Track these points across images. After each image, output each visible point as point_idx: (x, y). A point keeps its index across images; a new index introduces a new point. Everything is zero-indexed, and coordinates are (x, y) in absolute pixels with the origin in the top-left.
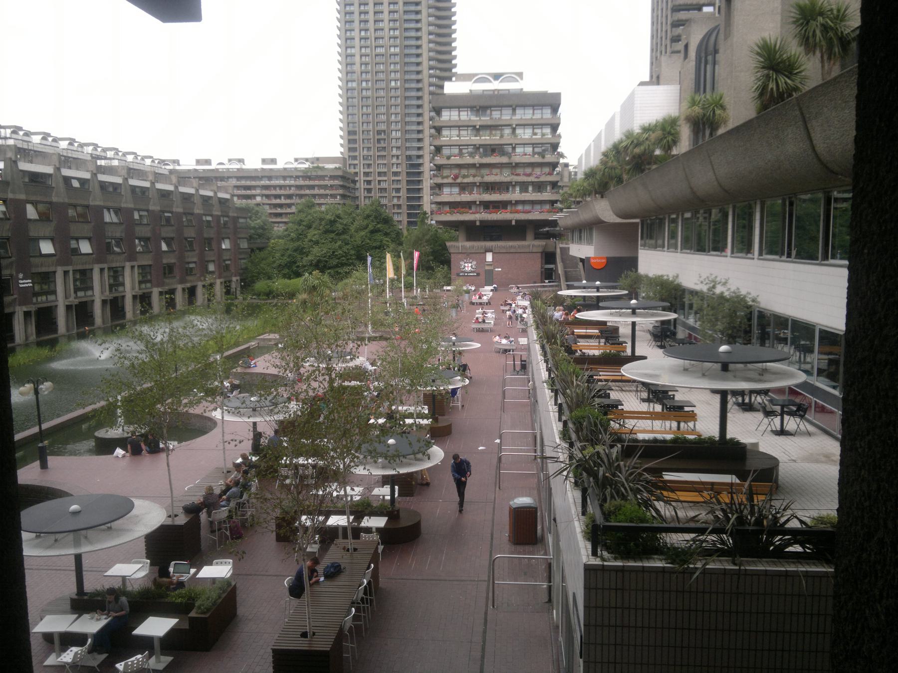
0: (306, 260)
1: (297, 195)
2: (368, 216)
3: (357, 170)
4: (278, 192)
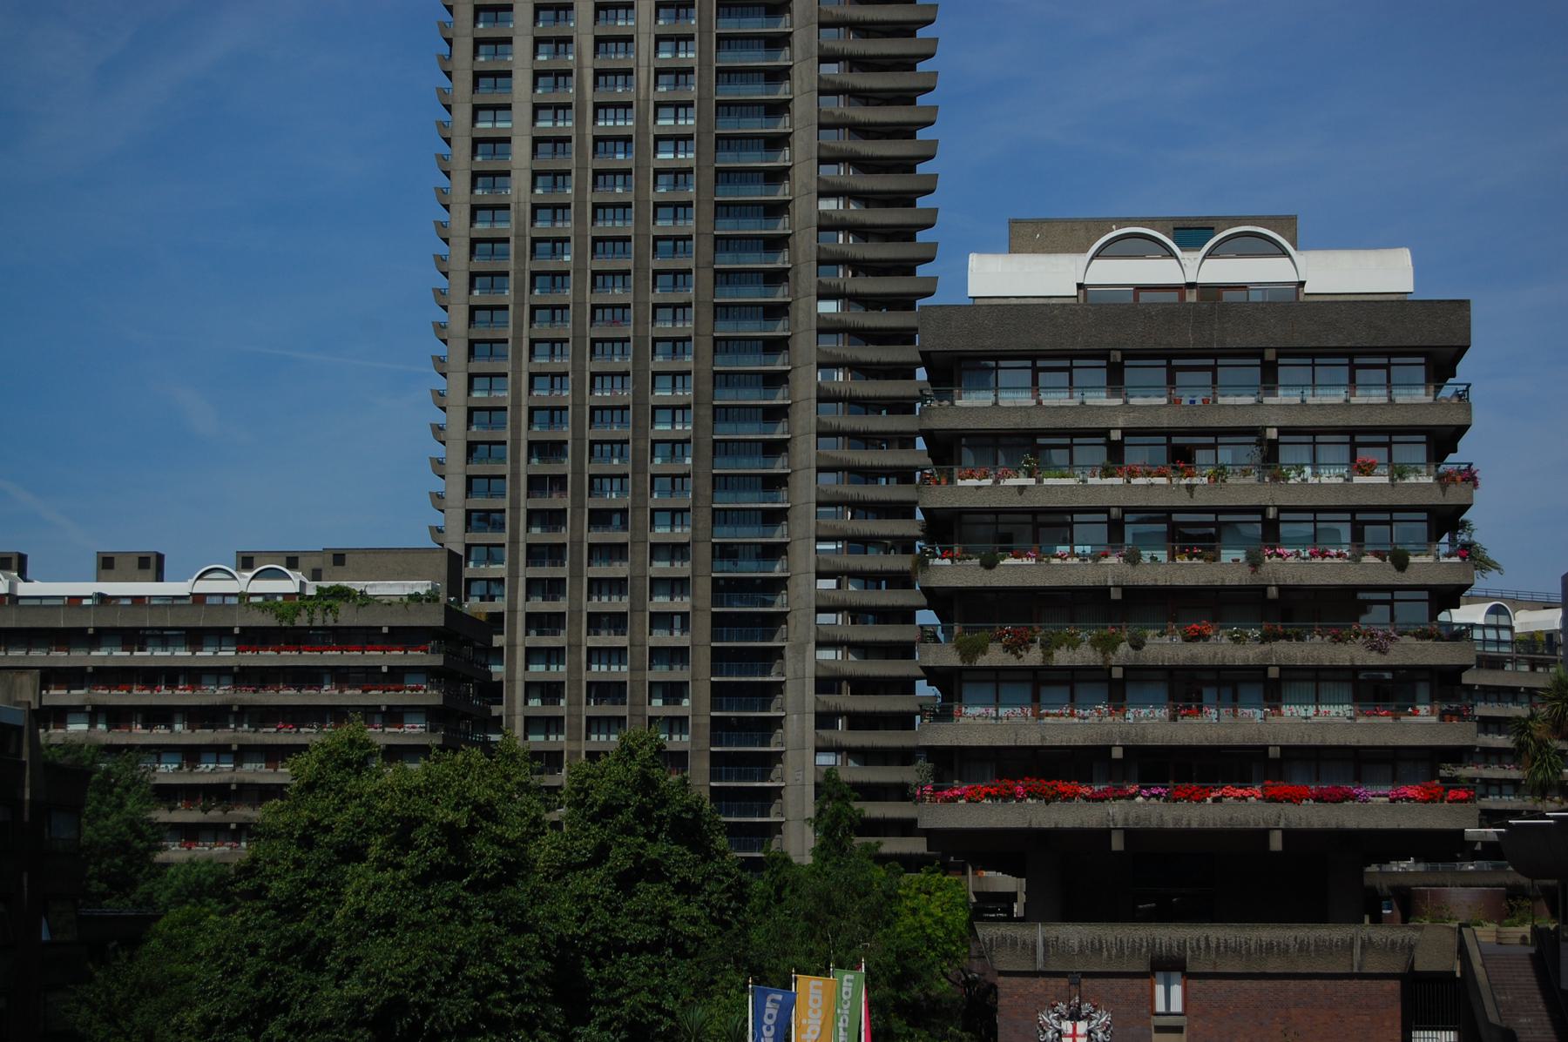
2: (610, 809)
3: (500, 605)
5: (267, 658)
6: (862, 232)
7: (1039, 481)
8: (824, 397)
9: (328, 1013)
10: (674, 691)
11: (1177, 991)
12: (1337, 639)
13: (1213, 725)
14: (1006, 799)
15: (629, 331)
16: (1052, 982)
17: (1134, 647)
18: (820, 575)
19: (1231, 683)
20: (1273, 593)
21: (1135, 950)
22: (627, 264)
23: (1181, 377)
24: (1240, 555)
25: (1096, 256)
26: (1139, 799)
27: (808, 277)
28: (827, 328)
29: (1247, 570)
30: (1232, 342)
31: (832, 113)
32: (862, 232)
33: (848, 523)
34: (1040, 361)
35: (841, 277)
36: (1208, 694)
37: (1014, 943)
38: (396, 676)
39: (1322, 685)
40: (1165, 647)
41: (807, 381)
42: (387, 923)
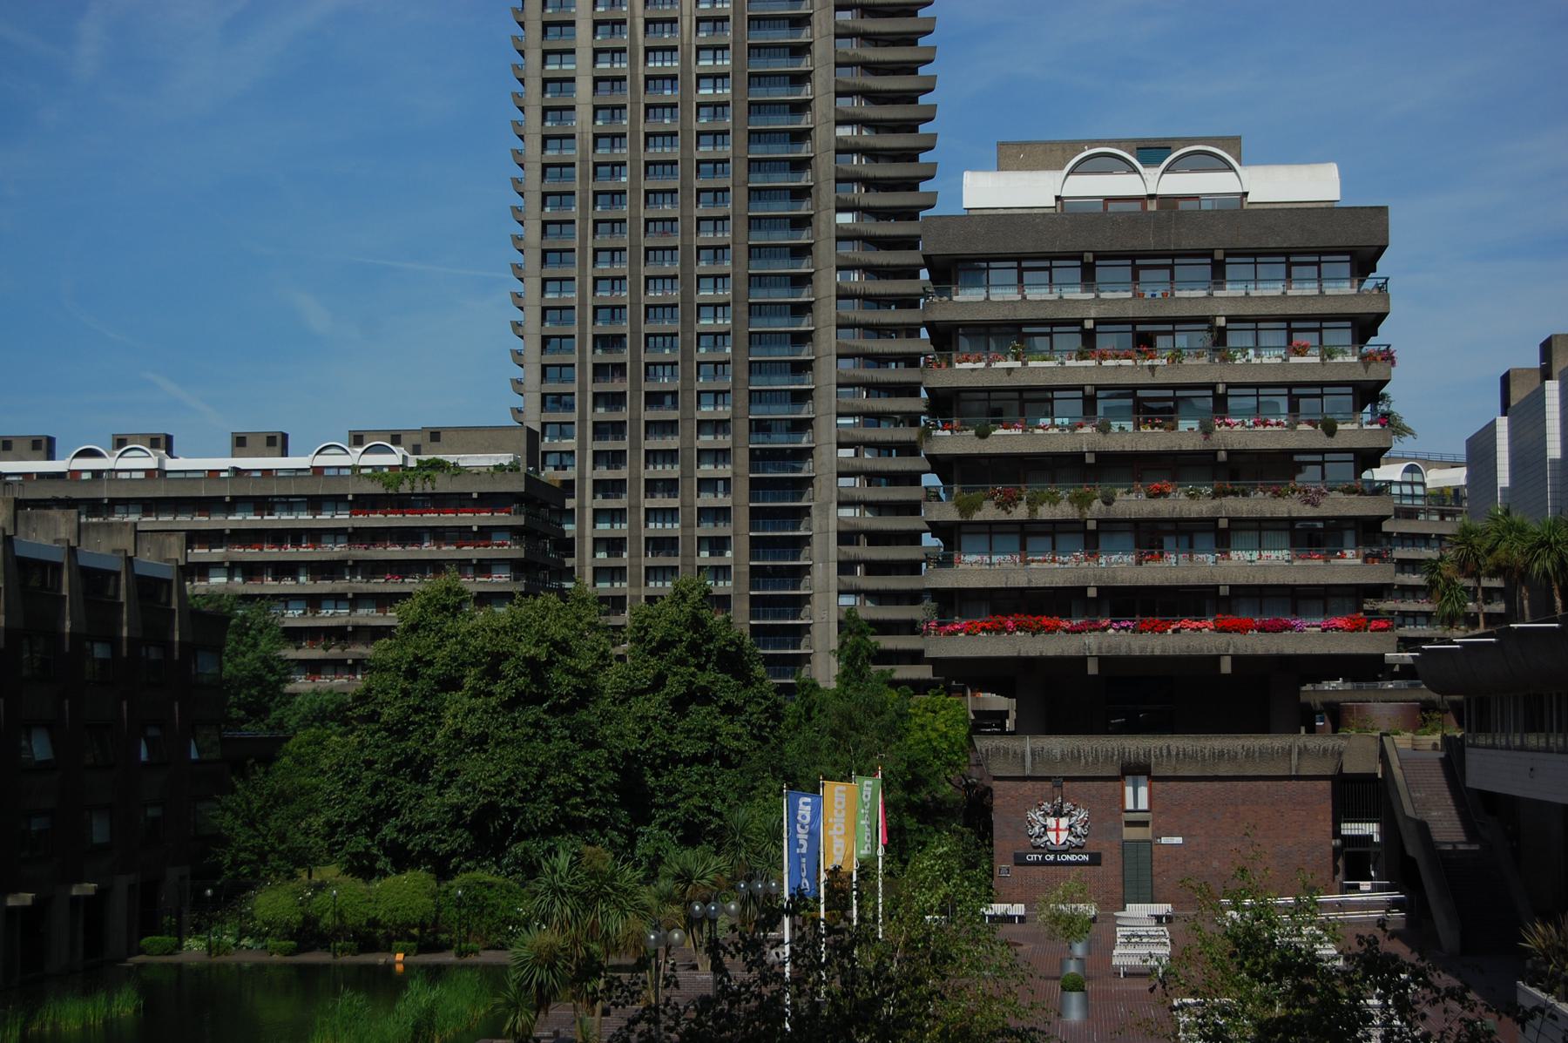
0: (434, 804)
1: (357, 563)
2: (665, 645)
3: (571, 474)
4: (289, 553)
5: (377, 520)
6: (873, 154)
7: (1024, 364)
8: (843, 295)
9: (431, 817)
10: (718, 545)
11: (1143, 792)
12: (1277, 494)
14: (998, 632)
15: (678, 242)
16: (1039, 785)
17: (1108, 502)
18: (840, 445)
19: (1187, 532)
20: (1222, 456)
21: (1108, 758)
22: (675, 184)
23: (1143, 274)
24: (1195, 424)
25: (1072, 172)
26: (1111, 631)
27: (827, 193)
28: (844, 236)
29: (1201, 437)
30: (1187, 244)
31: (846, 54)
32: (873, 154)
33: (865, 401)
34: (1023, 263)
35: (856, 193)
36: (1168, 542)
37: (1006, 752)
38: (485, 534)
39: (1264, 533)
40: (1131, 503)
41: (828, 281)
42: (480, 741)
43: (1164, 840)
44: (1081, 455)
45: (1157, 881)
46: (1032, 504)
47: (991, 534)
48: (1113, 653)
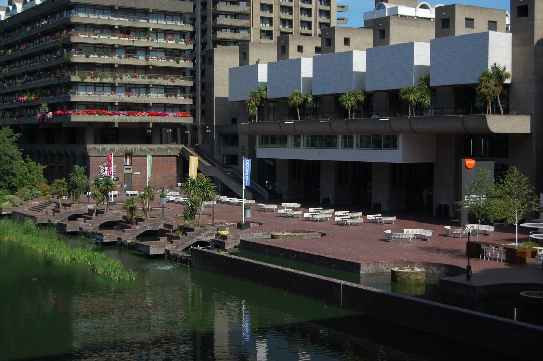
11: (128, 160)
12: (164, 79)
13: (134, 98)
14: (90, 114)
16: (102, 158)
17: (121, 78)
19: (137, 87)
20: (151, 67)
24: (144, 58)
36: (133, 90)
37: (95, 149)
40: (127, 79)
43: (135, 173)
44: (114, 64)
45: (133, 184)
46: (101, 78)
47: (103, 87)
48: (122, 121)
